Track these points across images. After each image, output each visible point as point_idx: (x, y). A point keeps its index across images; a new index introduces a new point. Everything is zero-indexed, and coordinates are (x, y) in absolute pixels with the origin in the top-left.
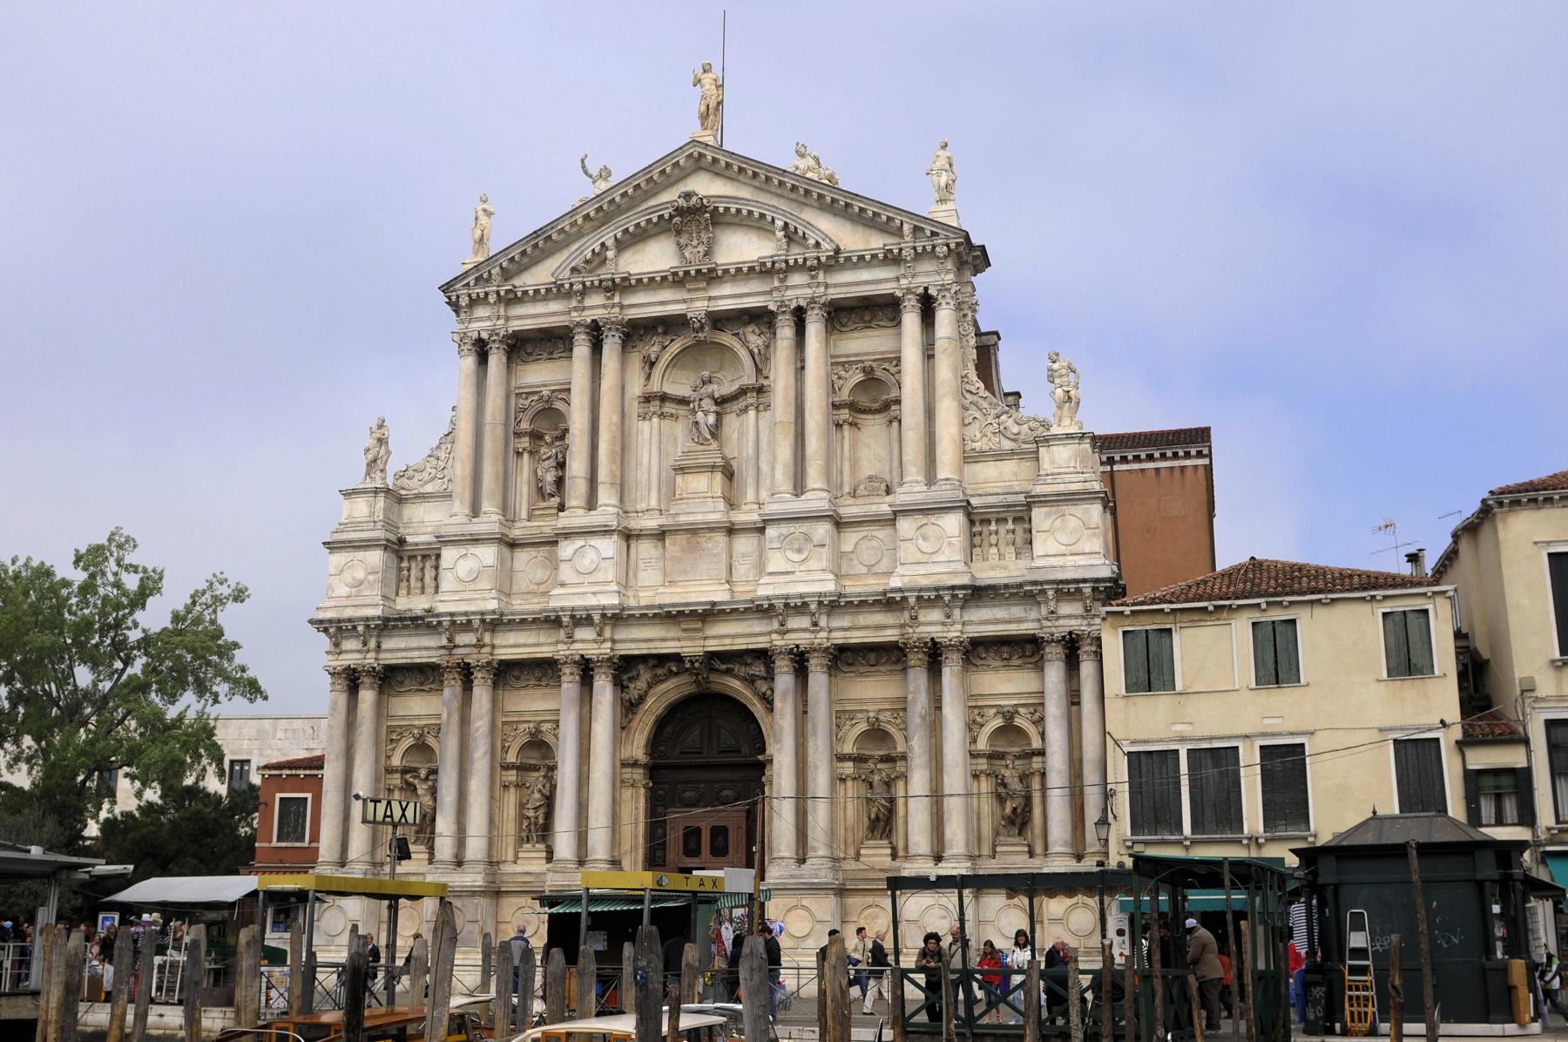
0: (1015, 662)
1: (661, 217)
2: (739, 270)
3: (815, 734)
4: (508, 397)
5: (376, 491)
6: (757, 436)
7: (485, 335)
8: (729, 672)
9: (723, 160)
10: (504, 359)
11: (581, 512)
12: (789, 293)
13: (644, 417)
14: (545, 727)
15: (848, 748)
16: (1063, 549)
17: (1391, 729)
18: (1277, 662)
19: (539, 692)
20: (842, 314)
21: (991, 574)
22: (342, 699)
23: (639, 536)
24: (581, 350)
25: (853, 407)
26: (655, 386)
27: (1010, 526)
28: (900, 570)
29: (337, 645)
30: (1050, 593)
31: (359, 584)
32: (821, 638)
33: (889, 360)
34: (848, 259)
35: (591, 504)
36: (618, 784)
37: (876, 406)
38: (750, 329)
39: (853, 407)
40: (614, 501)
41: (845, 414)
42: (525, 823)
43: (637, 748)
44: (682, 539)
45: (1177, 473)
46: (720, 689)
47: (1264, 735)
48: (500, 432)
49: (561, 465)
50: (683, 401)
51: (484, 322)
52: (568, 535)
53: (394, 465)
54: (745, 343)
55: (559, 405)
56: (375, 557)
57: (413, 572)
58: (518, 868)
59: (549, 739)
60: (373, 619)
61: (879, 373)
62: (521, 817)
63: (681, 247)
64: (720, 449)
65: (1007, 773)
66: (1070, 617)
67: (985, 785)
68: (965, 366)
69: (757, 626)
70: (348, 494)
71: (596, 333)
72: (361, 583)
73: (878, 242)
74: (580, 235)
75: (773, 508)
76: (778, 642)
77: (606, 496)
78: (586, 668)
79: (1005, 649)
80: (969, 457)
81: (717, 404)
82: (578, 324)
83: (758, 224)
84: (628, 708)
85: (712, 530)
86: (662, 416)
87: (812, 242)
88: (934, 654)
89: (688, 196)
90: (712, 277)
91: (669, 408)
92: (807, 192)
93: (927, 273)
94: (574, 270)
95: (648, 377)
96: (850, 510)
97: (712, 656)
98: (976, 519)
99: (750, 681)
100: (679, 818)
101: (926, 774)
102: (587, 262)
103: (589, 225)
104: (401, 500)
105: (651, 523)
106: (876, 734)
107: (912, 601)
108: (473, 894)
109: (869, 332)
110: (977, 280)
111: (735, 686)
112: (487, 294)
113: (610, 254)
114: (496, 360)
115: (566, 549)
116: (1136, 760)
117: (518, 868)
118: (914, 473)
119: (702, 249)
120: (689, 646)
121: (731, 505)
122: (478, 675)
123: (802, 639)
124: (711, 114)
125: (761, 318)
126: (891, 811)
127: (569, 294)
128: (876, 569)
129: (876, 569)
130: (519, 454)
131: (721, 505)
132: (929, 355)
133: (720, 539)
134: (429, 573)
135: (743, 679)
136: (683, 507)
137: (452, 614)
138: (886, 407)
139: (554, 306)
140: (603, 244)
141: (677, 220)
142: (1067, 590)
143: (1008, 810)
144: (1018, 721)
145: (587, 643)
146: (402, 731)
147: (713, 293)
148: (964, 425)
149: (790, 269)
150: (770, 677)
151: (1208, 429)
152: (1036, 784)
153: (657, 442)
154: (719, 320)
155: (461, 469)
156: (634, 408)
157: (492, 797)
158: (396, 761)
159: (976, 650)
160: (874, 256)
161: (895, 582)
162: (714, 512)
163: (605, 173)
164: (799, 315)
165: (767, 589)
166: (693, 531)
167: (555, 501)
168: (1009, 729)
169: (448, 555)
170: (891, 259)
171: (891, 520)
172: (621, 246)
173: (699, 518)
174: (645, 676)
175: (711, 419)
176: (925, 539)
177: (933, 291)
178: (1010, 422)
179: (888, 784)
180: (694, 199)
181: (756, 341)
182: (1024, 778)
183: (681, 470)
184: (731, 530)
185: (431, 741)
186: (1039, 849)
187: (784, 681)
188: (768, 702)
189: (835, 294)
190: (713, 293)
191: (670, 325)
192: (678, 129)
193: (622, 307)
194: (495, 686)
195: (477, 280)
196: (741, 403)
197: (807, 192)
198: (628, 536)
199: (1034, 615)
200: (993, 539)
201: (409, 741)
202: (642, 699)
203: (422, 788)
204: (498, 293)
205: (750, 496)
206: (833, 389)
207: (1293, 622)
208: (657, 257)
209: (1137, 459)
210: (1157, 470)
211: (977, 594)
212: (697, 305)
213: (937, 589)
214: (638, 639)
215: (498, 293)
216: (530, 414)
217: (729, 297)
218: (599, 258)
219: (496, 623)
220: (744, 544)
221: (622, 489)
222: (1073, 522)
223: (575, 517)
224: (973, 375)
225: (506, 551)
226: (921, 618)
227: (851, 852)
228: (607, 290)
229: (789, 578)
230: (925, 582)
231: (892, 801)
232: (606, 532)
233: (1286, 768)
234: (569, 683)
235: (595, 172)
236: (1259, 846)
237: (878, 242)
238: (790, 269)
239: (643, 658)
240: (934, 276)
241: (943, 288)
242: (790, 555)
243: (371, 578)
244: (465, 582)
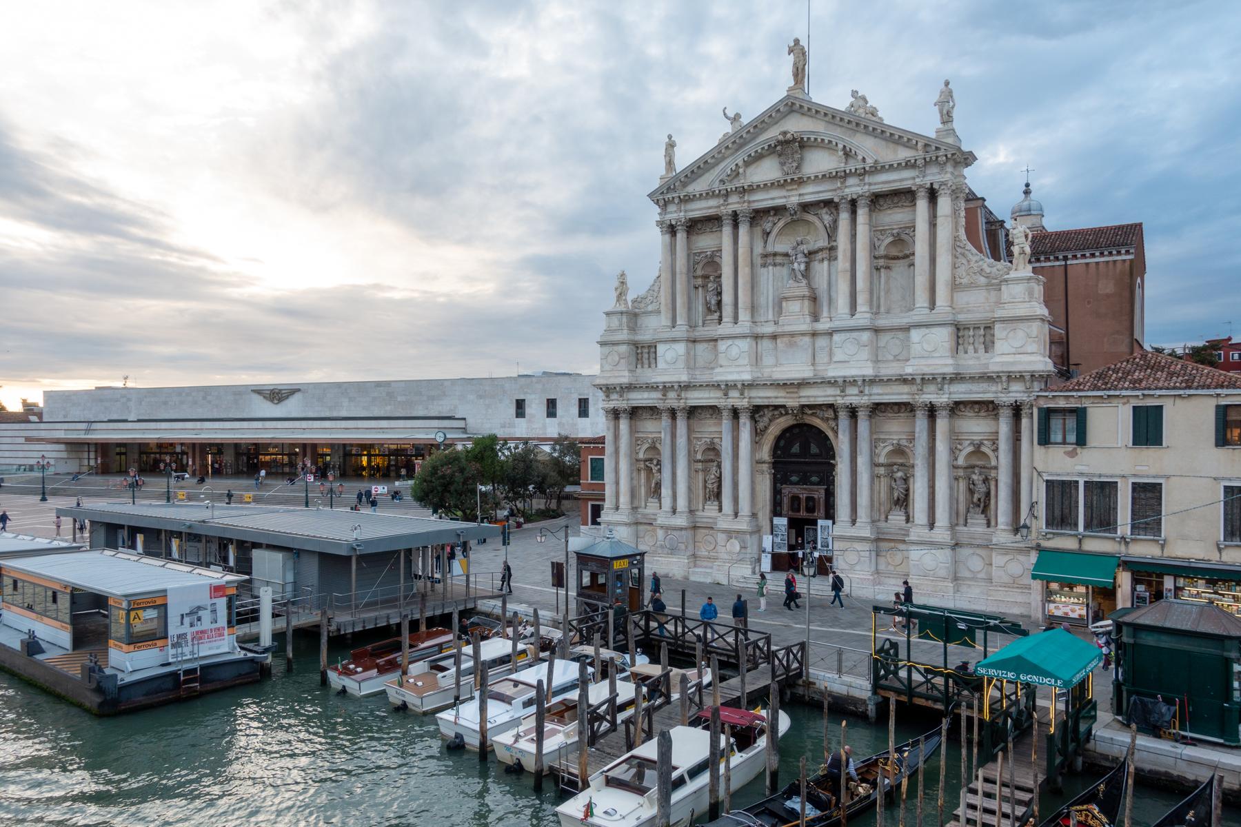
0: (983, 414)
4: (689, 255)
5: (622, 313)
6: (832, 277)
8: (813, 414)
9: (806, 106)
10: (685, 235)
11: (731, 325)
12: (847, 191)
13: (764, 265)
14: (716, 440)
15: (882, 460)
16: (1013, 350)
17: (1223, 479)
18: (1148, 428)
19: (711, 422)
20: (877, 200)
21: (971, 362)
22: (612, 424)
24: (727, 230)
25: (886, 257)
26: (770, 249)
27: (982, 332)
28: (912, 362)
29: (608, 396)
30: (1004, 379)
32: (865, 400)
33: (909, 228)
34: (883, 167)
35: (736, 320)
36: (753, 474)
38: (824, 210)
39: (886, 257)
40: (748, 317)
41: (881, 262)
43: (765, 453)
44: (786, 339)
45: (1111, 265)
47: (1135, 475)
48: (684, 277)
49: (720, 294)
50: (787, 255)
51: (676, 214)
52: (722, 339)
53: (630, 297)
54: (821, 219)
55: (717, 259)
56: (623, 349)
57: (646, 356)
58: (706, 514)
59: (718, 447)
61: (903, 236)
62: (705, 487)
63: (783, 164)
64: (809, 285)
65: (975, 477)
66: (1017, 393)
67: (962, 485)
68: (957, 230)
69: (831, 391)
70: (608, 314)
74: (724, 159)
75: (837, 324)
76: (840, 401)
77: (744, 316)
78: (735, 413)
79: (977, 406)
80: (955, 286)
81: (806, 256)
85: (803, 334)
86: (775, 265)
87: (860, 157)
88: (932, 411)
89: (785, 133)
90: (801, 182)
91: (779, 259)
92: (857, 124)
93: (933, 174)
94: (722, 182)
95: (766, 242)
97: (803, 406)
98: (959, 330)
100: (787, 490)
101: (926, 479)
103: (729, 152)
104: (636, 315)
105: (769, 329)
106: (899, 451)
107: (919, 381)
108: (681, 529)
109: (897, 210)
110: (967, 171)
111: (817, 422)
113: (741, 170)
114: (681, 236)
115: (722, 346)
116: (1050, 484)
117: (706, 514)
118: (922, 299)
119: (795, 164)
121: (815, 317)
122: (679, 414)
124: (799, 73)
126: (907, 495)
127: (718, 196)
131: (808, 319)
132: (933, 225)
133: (807, 339)
134: (652, 355)
135: (822, 419)
138: (906, 257)
139: (713, 202)
141: (779, 148)
142: (1011, 377)
143: (975, 500)
144: (984, 449)
145: (735, 399)
146: (644, 440)
147: (802, 191)
148: (954, 267)
149: (846, 175)
150: (836, 418)
151: (1140, 225)
152: (993, 484)
153: (771, 279)
154: (805, 207)
155: (664, 297)
156: (758, 261)
157: (689, 476)
158: (641, 456)
159: (956, 408)
160: (899, 164)
161: (909, 370)
162: (805, 325)
163: (737, 117)
164: (853, 203)
165: (833, 372)
167: (716, 316)
168: (977, 451)
169: (661, 348)
170: (909, 165)
171: (907, 329)
172: (747, 164)
174: (768, 414)
175: (803, 267)
179: (906, 480)
181: (827, 219)
182: (986, 480)
184: (814, 334)
185: (658, 445)
186: (993, 523)
187: (844, 421)
188: (836, 432)
190: (802, 191)
191: (778, 210)
193: (749, 202)
194: (688, 418)
196: (820, 256)
197: (857, 124)
198: (757, 337)
199: (994, 388)
200: (971, 340)
201: (647, 446)
202: (766, 428)
203: (655, 469)
205: (825, 314)
206: (873, 247)
207: (1161, 407)
208: (768, 170)
209: (1084, 256)
210: (1097, 263)
211: (957, 378)
212: (792, 198)
214: (763, 396)
216: (701, 265)
217: (811, 193)
218: (736, 174)
219: (687, 387)
220: (822, 342)
221: (753, 309)
222: (1020, 334)
224: (963, 236)
225: (691, 345)
227: (883, 517)
228: (740, 193)
230: (927, 370)
231: (907, 490)
233: (1148, 496)
234: (726, 423)
235: (731, 114)
236: (1127, 543)
237: (904, 154)
238: (846, 175)
239: (768, 406)
240: (933, 176)
241: (943, 184)
244: (671, 364)
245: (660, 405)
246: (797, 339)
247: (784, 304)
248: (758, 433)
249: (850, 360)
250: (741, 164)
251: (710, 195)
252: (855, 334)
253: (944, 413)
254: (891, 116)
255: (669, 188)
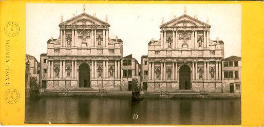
73: (201, 25)
111: (188, 64)
125: (191, 32)
145: (175, 60)
154: (187, 31)
188: (192, 66)
192: (182, 14)
237: (201, 25)
248: (178, 66)
254: (200, 19)
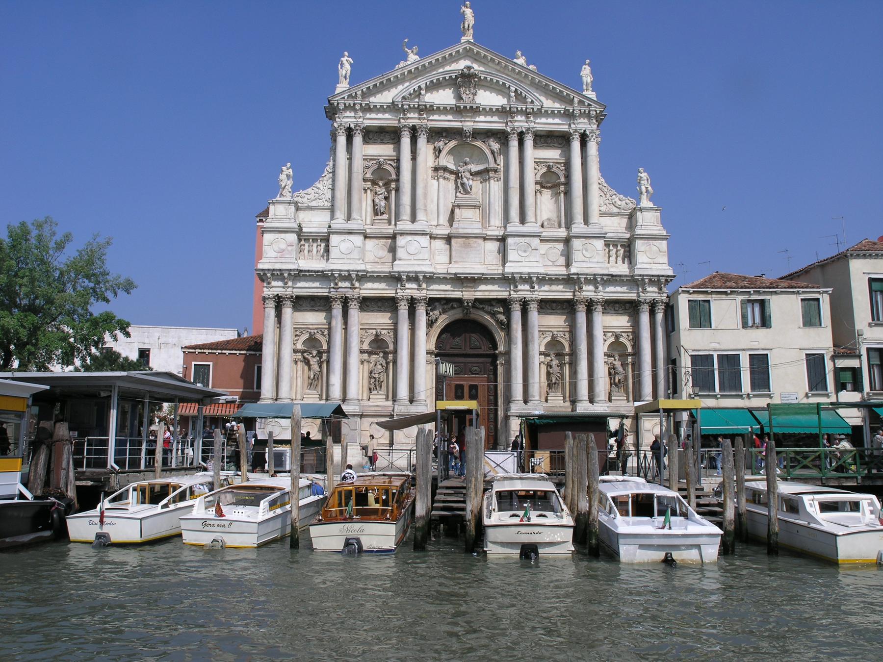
1: (450, 77)
2: (491, 109)
3: (533, 341)
7: (352, 126)
23: (435, 238)
31: (282, 251)
34: (546, 111)
37: (549, 185)
42: (373, 380)
44: (459, 240)
46: (480, 319)
52: (402, 234)
60: (294, 270)
71: (414, 132)
72: (284, 250)
73: (557, 106)
82: (405, 126)
83: (502, 89)
84: (430, 324)
86: (444, 178)
88: (590, 305)
94: (404, 98)
96: (546, 234)
97: (480, 303)
99: (493, 315)
102: (410, 94)
112: (354, 104)
113: (423, 92)
120: (468, 294)
123: (528, 295)
125: (502, 137)
128: (556, 263)
129: (556, 263)
130: (365, 191)
135: (489, 313)
136: (461, 225)
137: (340, 271)
140: (419, 87)
154: (478, 134)
156: (430, 172)
166: (466, 237)
173: (469, 231)
176: (586, 250)
177: (588, 132)
178: (617, 199)
180: (472, 70)
183: (459, 206)
189: (539, 127)
190: (477, 119)
195: (348, 96)
204: (361, 104)
212: (468, 125)
213: (595, 275)
215: (361, 104)
217: (484, 122)
218: (418, 93)
223: (405, 225)
226: (584, 288)
229: (520, 264)
230: (588, 271)
232: (424, 234)
242: (520, 252)
243: (290, 248)
245: (333, 294)
246: (472, 241)
247: (457, 211)
249: (532, 259)
250: (423, 86)
251: (393, 107)
252: (527, 240)
253: (600, 308)
255: (350, 96)
